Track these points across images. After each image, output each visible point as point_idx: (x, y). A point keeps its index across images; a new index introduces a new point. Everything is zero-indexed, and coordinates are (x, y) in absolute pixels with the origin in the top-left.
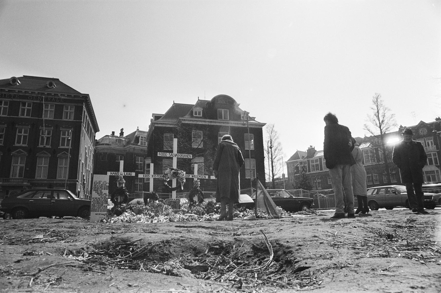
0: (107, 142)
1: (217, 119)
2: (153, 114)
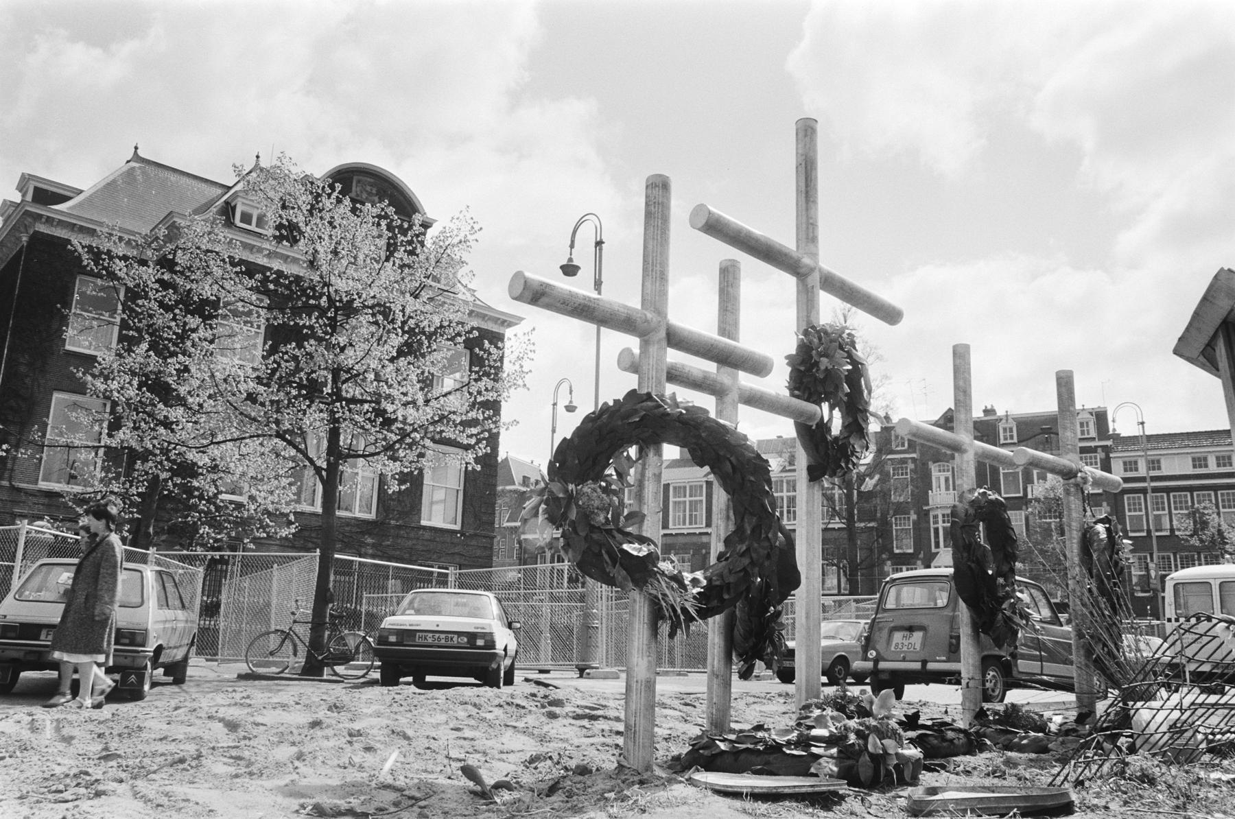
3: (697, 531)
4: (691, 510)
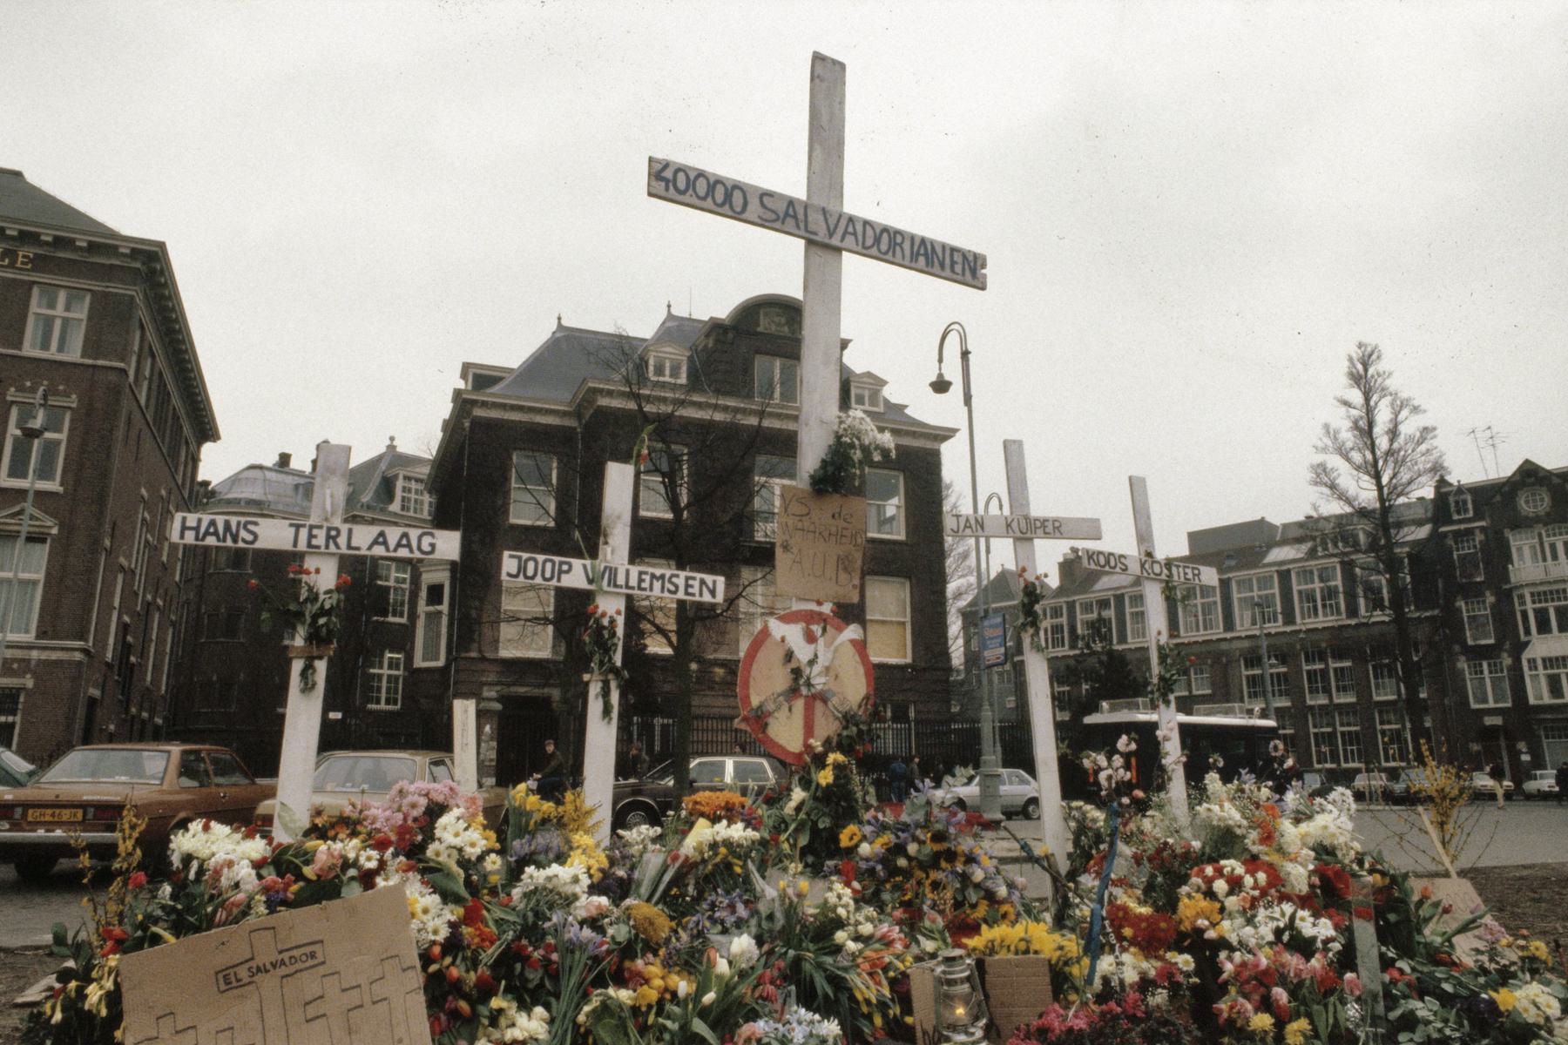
0: (255, 493)
1: (749, 396)
2: (466, 367)
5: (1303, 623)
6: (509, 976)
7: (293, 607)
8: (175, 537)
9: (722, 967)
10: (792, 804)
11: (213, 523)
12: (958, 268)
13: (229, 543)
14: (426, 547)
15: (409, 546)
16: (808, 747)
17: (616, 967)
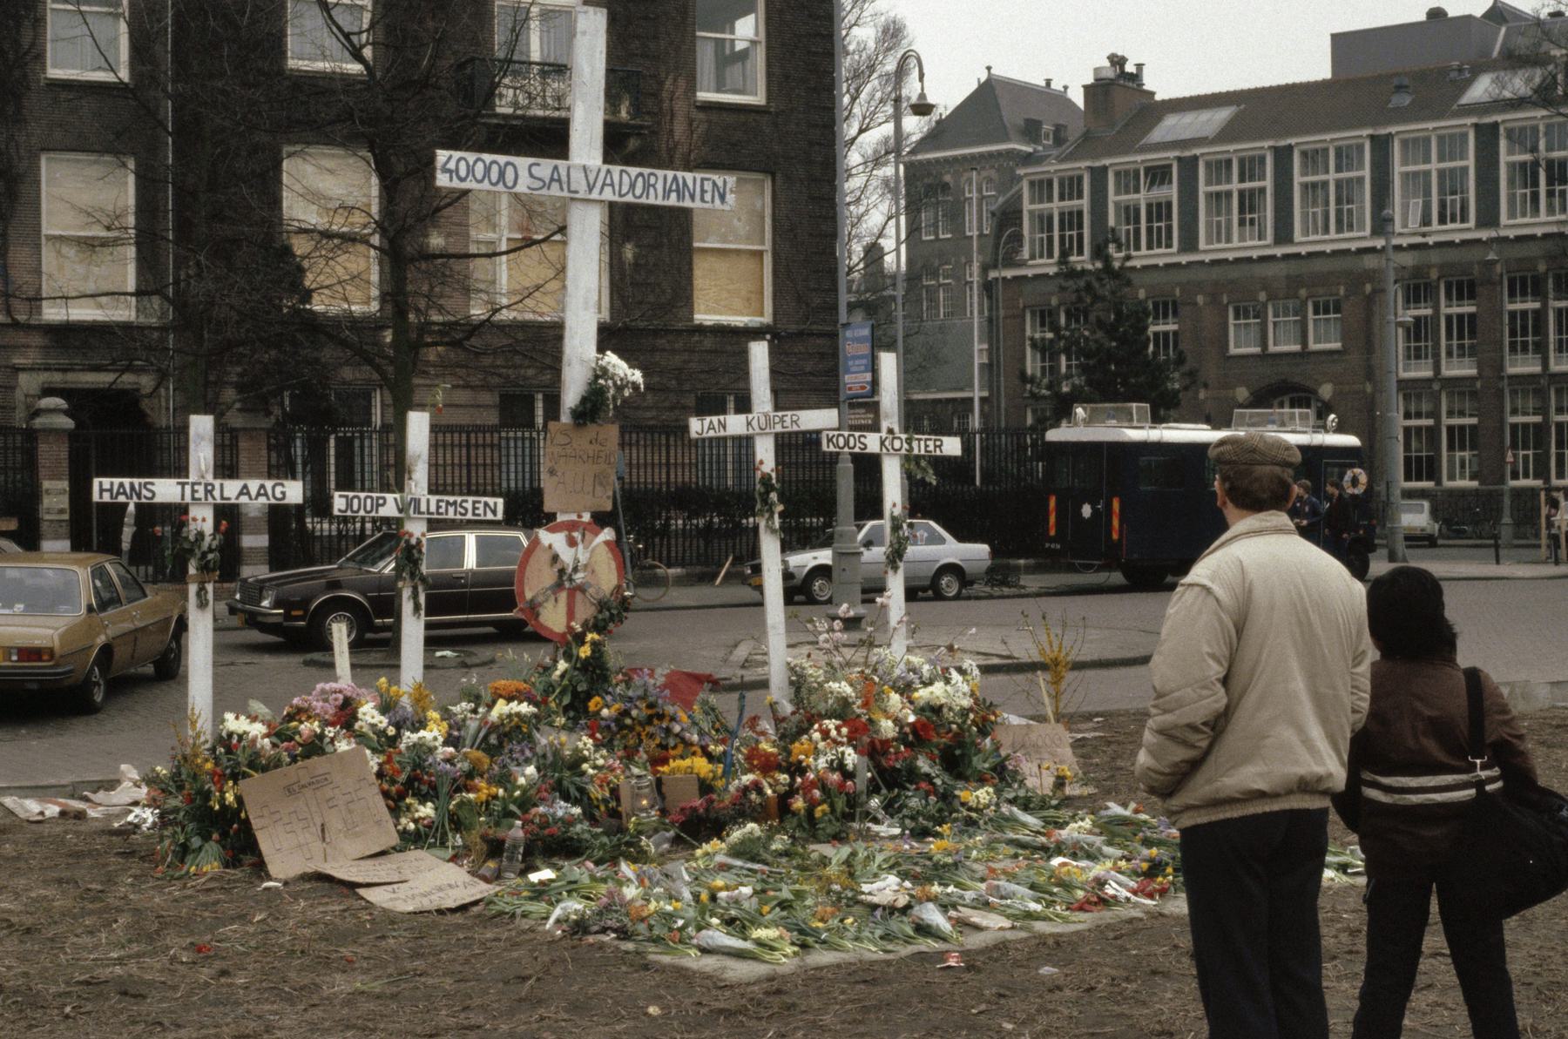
3: (1353, 246)
4: (1339, 201)
5: (1511, 225)
6: (412, 787)
7: (186, 546)
8: (96, 497)
9: (522, 781)
10: (558, 673)
11: (121, 485)
12: (708, 197)
13: (135, 499)
14: (279, 495)
15: (266, 494)
16: (570, 628)
17: (463, 783)
